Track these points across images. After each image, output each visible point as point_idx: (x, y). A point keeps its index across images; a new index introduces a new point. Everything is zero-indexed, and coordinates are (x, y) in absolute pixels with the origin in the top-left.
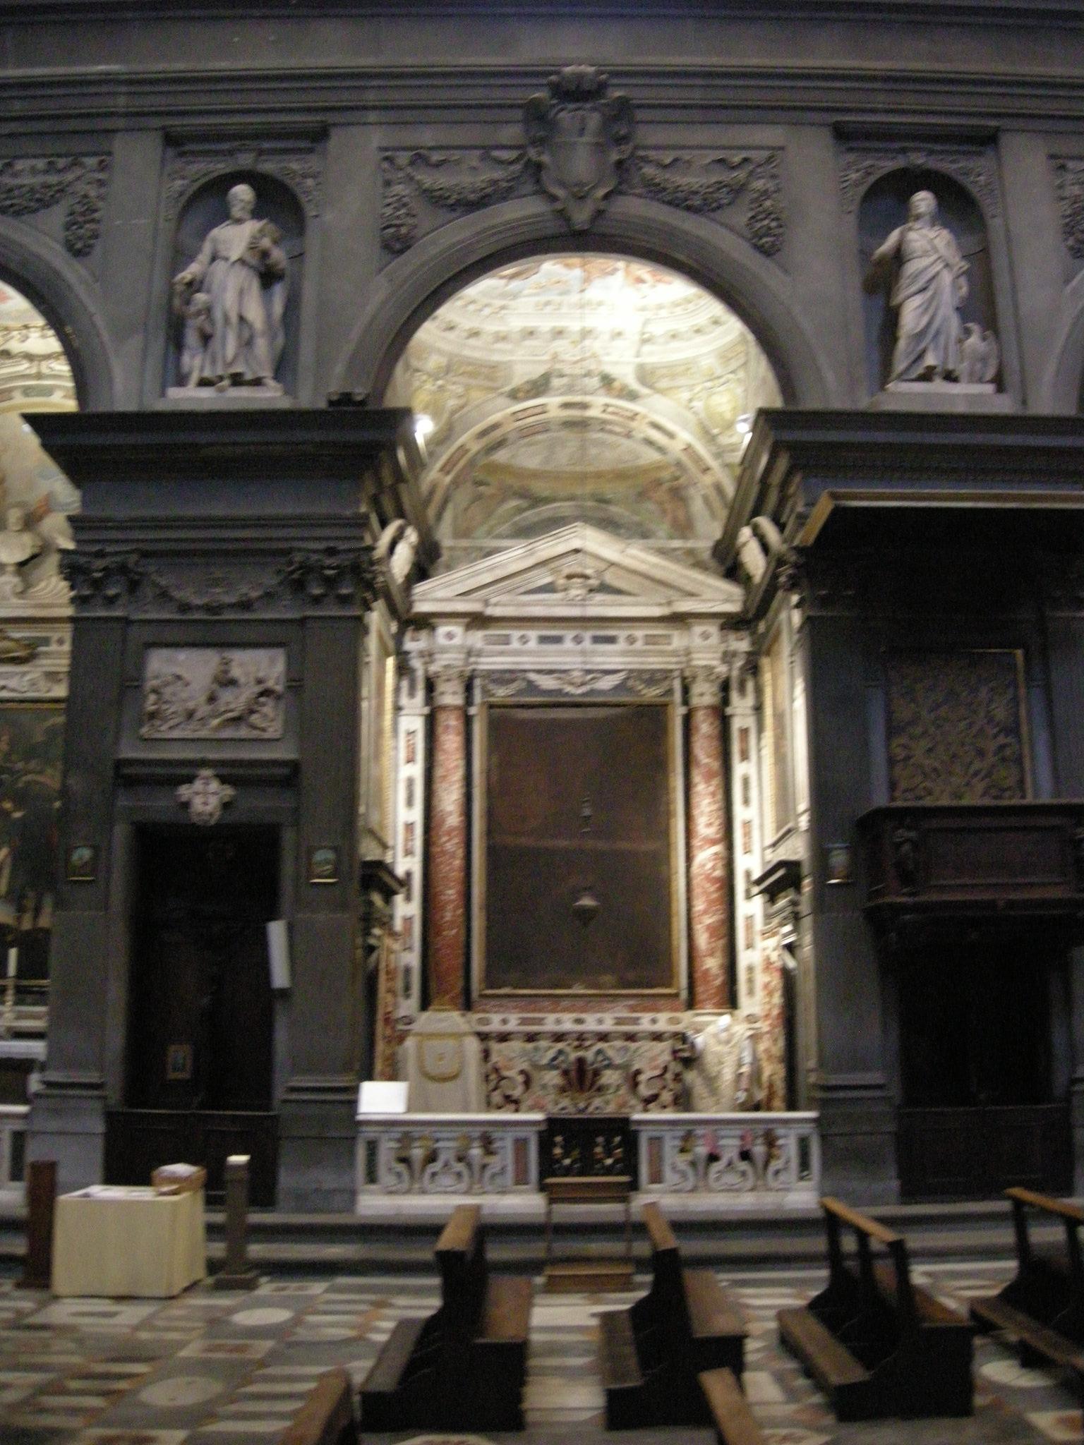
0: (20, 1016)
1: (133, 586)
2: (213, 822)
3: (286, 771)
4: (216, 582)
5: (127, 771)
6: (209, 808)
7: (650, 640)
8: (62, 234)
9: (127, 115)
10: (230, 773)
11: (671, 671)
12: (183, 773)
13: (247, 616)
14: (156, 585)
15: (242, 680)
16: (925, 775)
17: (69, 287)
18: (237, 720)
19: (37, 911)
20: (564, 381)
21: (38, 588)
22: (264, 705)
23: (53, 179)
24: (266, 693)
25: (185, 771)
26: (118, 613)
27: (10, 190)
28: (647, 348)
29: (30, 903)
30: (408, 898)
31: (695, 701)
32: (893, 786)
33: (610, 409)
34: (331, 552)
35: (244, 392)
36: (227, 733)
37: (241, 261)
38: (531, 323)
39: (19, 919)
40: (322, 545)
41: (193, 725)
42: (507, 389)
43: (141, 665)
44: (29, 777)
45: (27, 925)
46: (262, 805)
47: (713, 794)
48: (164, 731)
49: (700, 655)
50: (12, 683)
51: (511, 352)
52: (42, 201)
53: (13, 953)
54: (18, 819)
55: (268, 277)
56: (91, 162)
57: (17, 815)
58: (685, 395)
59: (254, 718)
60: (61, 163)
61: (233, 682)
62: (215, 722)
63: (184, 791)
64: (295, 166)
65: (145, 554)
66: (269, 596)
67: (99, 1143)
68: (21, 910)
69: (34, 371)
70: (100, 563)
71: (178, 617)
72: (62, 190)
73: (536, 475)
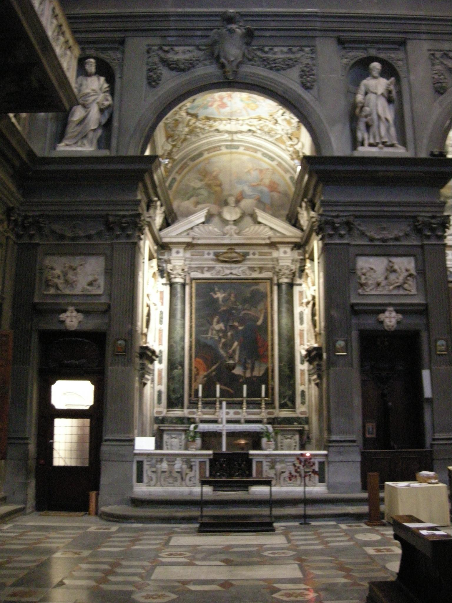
0: (204, 414)
3: (422, 308)
4: (384, 229)
5: (356, 308)
6: (392, 324)
7: (261, 254)
8: (299, 80)
9: (321, 30)
10: (400, 309)
12: (381, 309)
13: (398, 243)
14: (358, 229)
15: (399, 270)
17: (307, 103)
18: (398, 287)
19: (252, 369)
21: (245, 231)
22: (408, 280)
23: (291, 56)
24: (411, 275)
25: (382, 308)
26: (346, 241)
27: (275, 60)
29: (249, 366)
30: (160, 362)
34: (337, 216)
35: (390, 150)
36: (395, 292)
37: (382, 94)
39: (245, 373)
40: (430, 214)
41: (380, 289)
43: (355, 264)
44: (245, 312)
45: (248, 375)
46: (415, 322)
48: (368, 291)
49: (283, 261)
50: (234, 272)
52: (288, 65)
53: (245, 387)
54: (241, 330)
55: (390, 101)
56: (307, 49)
59: (406, 286)
60: (295, 49)
61: (395, 271)
62: (391, 287)
63: (382, 317)
64: (393, 55)
65: (356, 217)
66: (406, 235)
67: (359, 465)
68: (245, 368)
69: (229, 138)
71: (370, 243)
72: (296, 61)
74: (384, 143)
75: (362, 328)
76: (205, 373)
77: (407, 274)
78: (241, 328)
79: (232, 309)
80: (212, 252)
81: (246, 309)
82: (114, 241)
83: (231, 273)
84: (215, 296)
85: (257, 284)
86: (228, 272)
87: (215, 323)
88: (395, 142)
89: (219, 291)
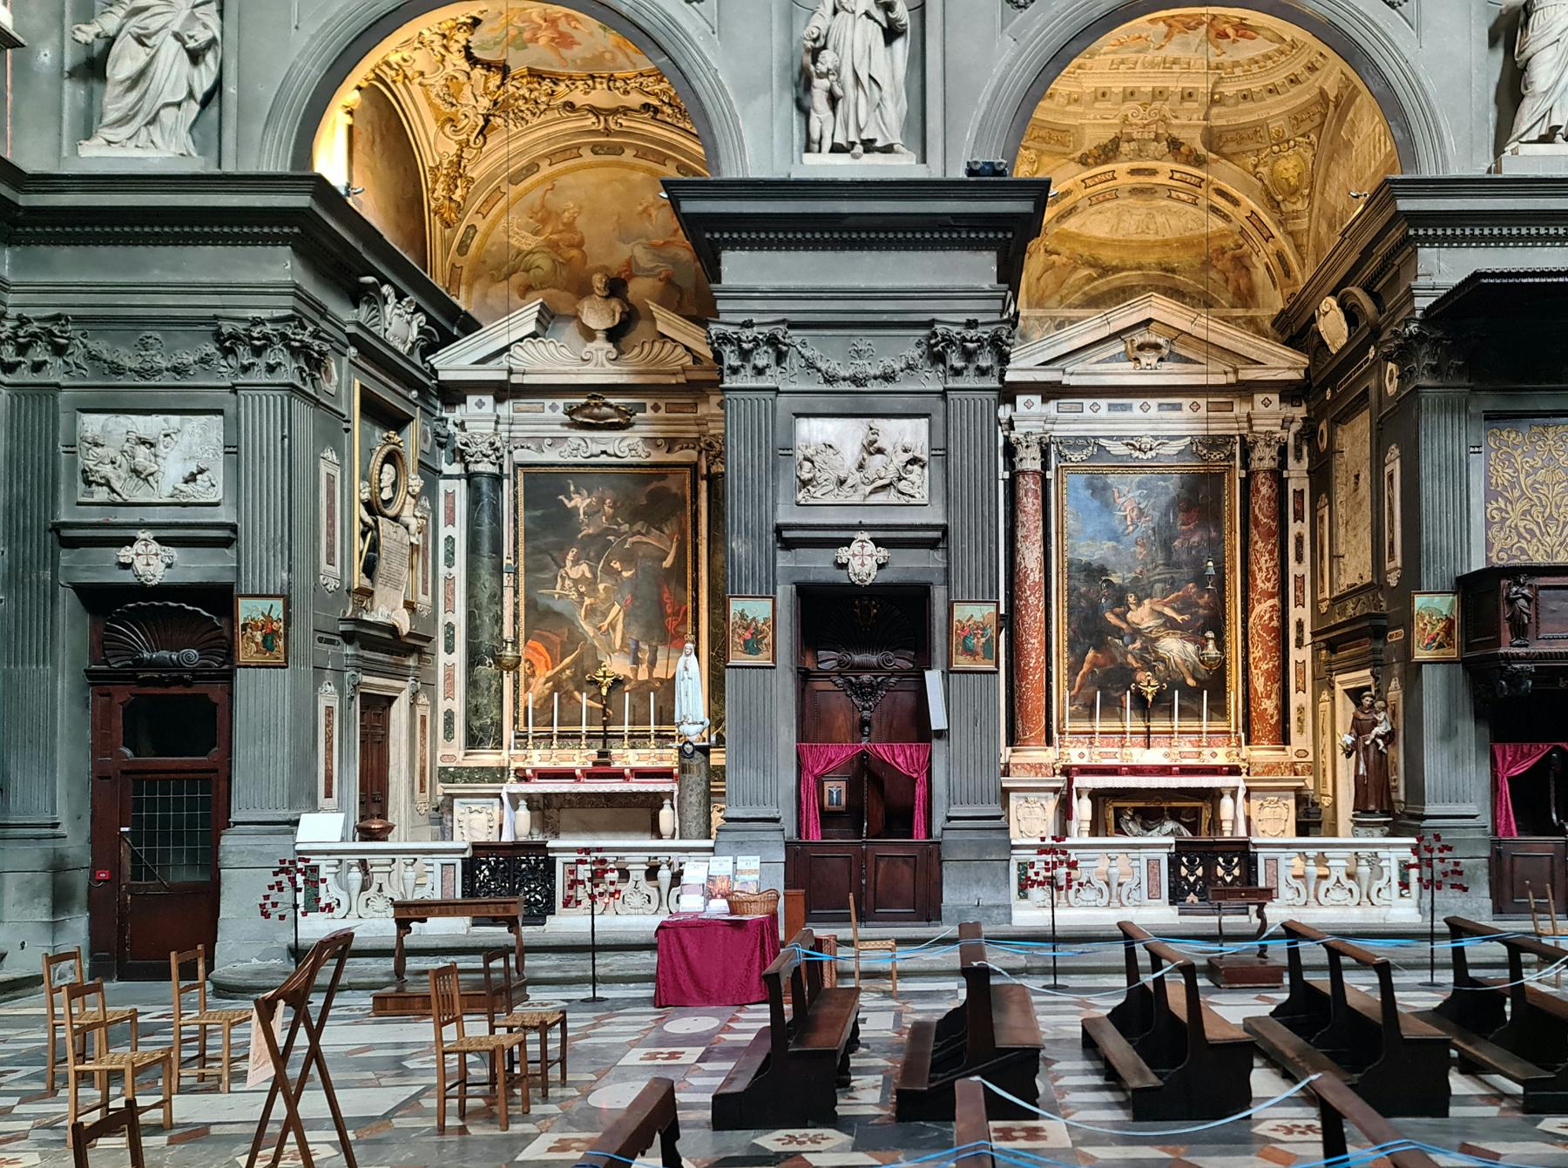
1: (780, 357)
2: (869, 581)
3: (937, 534)
5: (786, 534)
6: (866, 570)
11: (1233, 436)
13: (890, 387)
15: (889, 449)
16: (1520, 535)
20: (1133, 145)
22: (911, 472)
24: (914, 461)
28: (1215, 110)
31: (1255, 465)
32: (1489, 546)
33: (1177, 176)
38: (1103, 84)
40: (963, 318)
42: (1079, 154)
43: (791, 432)
47: (1271, 553)
48: (818, 494)
51: (1082, 115)
57: (626, 574)
58: (1253, 160)
59: (902, 485)
61: (880, 451)
70: (748, 333)
71: (826, 387)
73: (1103, 244)
74: (869, 146)
75: (801, 578)
76: (549, 673)
77: (907, 456)
78: (626, 574)
79: (607, 531)
80: (560, 402)
81: (639, 533)
82: (240, 381)
83: (604, 452)
84: (570, 505)
85: (663, 477)
86: (596, 449)
87: (569, 564)
88: (896, 140)
89: (577, 492)
